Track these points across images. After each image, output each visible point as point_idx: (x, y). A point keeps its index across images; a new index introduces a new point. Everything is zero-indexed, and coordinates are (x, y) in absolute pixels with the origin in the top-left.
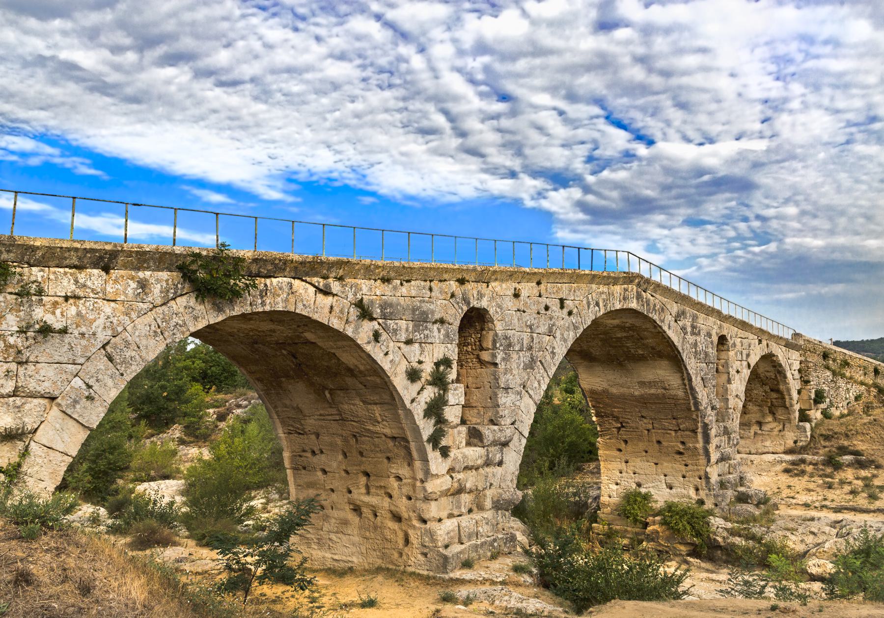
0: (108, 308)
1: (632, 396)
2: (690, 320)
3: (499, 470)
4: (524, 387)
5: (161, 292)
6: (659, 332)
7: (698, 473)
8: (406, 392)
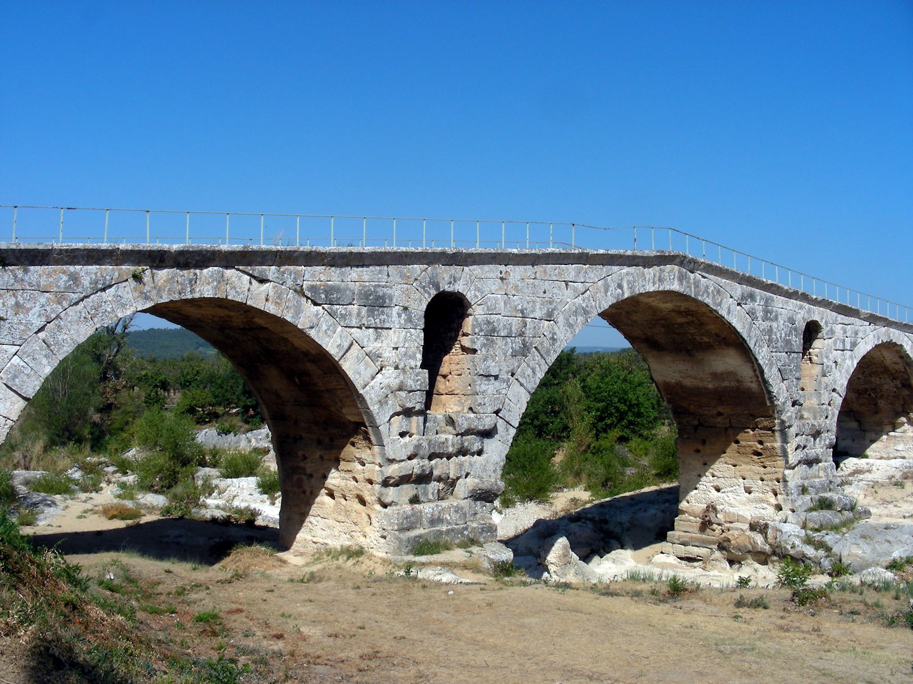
0: (43, 299)
1: (706, 389)
2: (762, 303)
4: (513, 375)
5: (91, 283)
6: (717, 318)
7: (776, 476)
8: (357, 376)
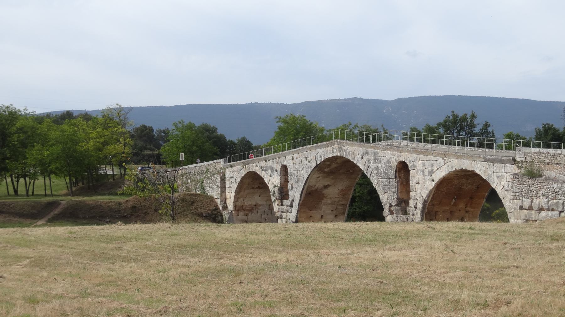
2: (373, 155)
3: (291, 214)
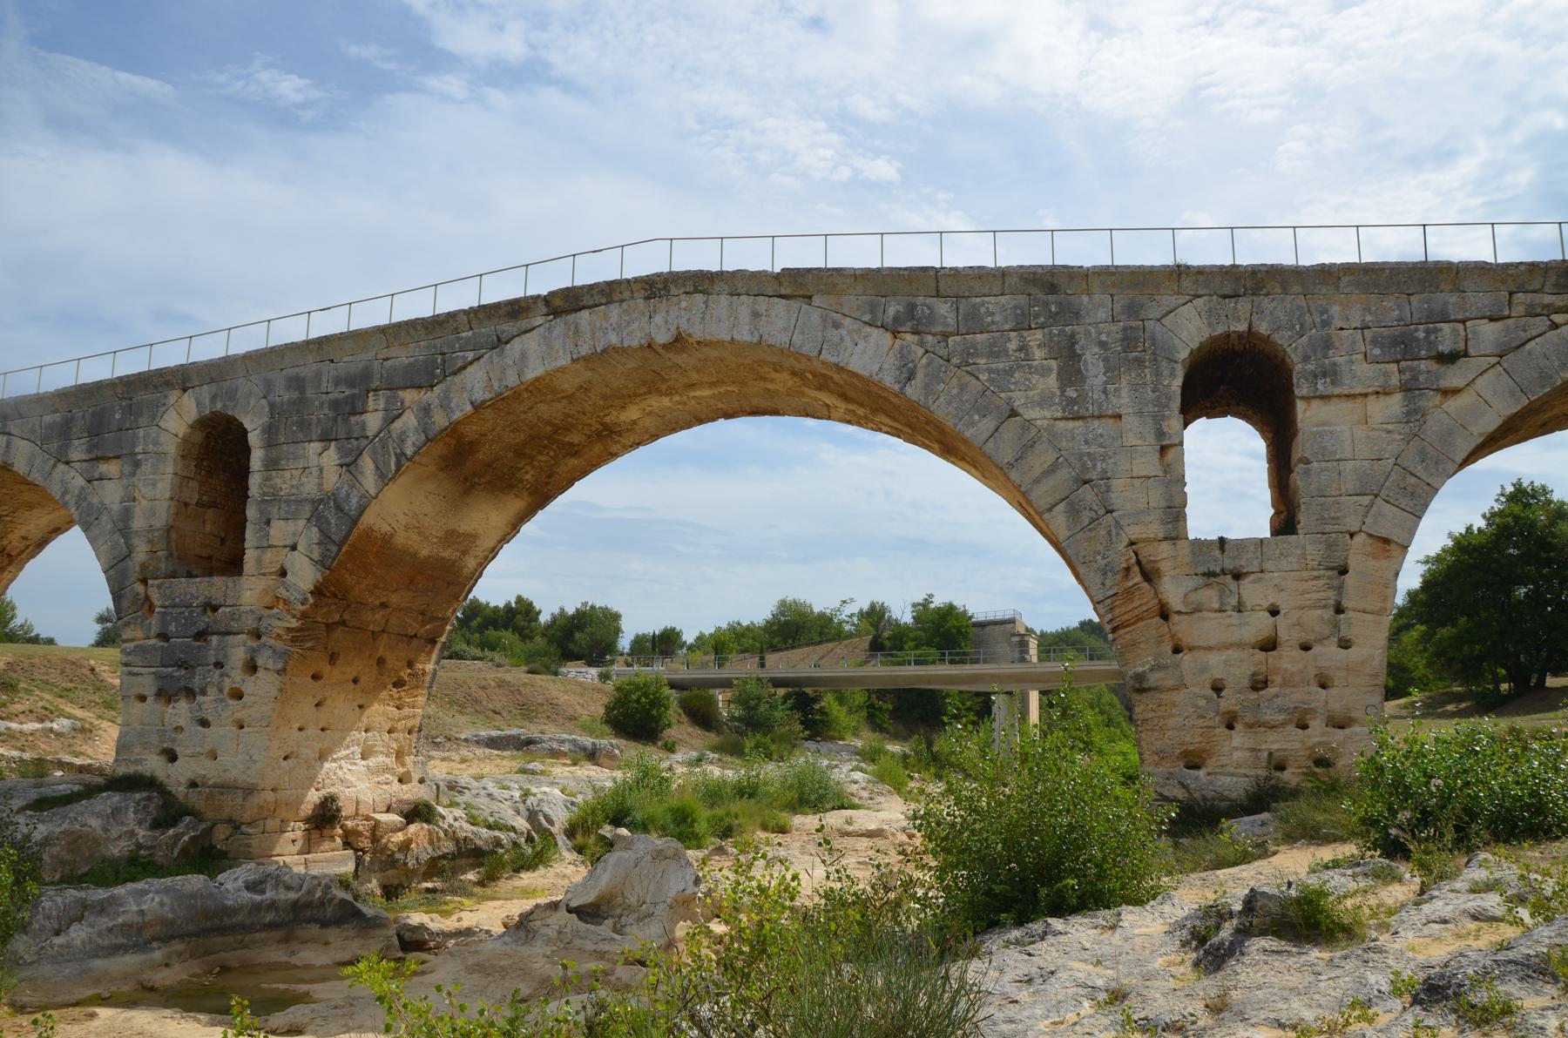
1: (414, 555)
